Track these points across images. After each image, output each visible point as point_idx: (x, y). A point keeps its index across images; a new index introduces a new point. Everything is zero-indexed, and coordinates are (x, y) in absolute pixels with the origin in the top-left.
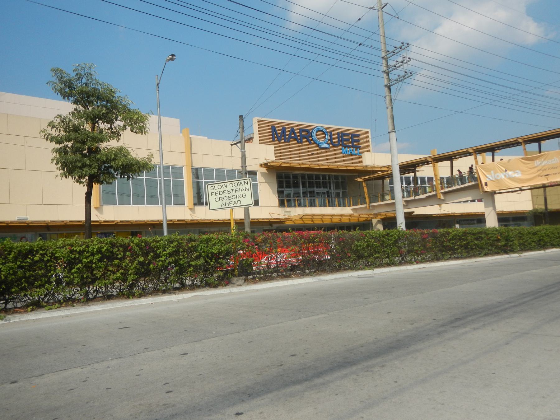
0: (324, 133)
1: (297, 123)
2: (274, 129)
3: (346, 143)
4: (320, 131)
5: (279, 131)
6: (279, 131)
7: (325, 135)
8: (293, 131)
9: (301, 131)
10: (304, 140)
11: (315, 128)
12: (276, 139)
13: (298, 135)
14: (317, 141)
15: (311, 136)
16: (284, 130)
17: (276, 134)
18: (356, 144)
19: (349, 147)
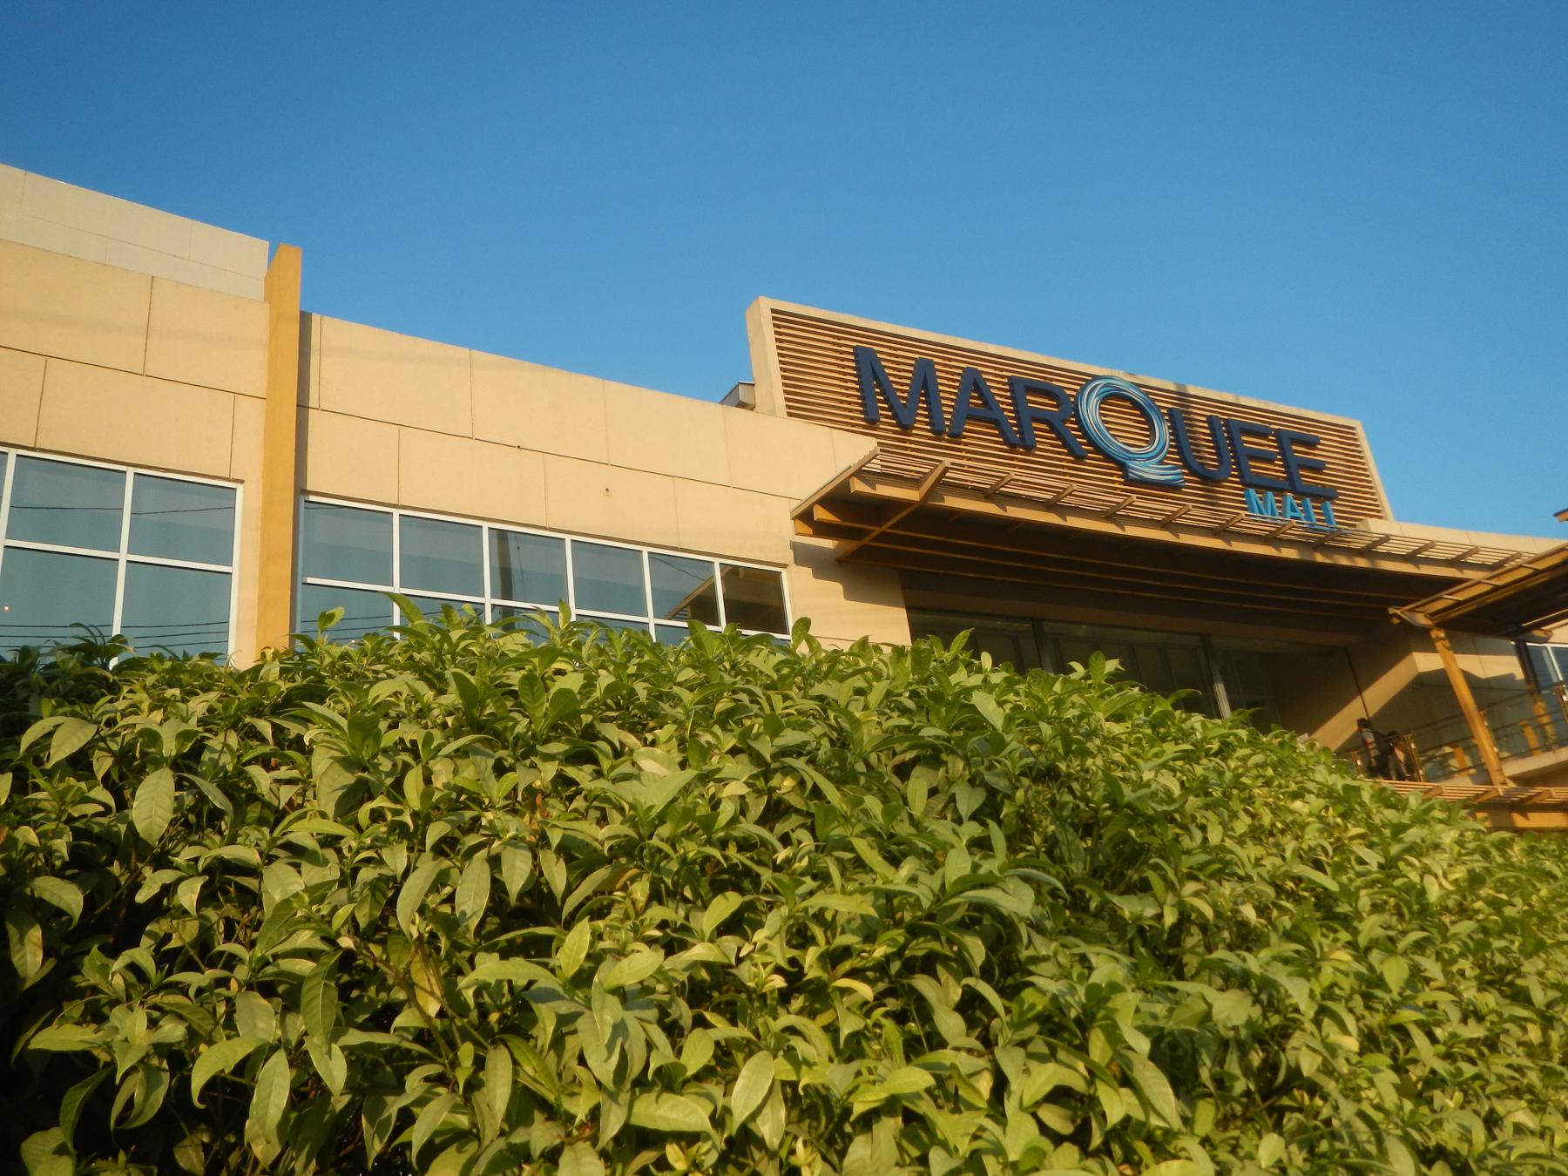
0: (1144, 413)
1: (992, 349)
2: (868, 368)
3: (1257, 468)
4: (1114, 397)
5: (901, 380)
6: (901, 380)
7: (1149, 421)
8: (973, 383)
9: (1022, 387)
10: (1045, 442)
11: (1091, 381)
12: (883, 409)
13: (1010, 411)
14: (1116, 445)
15: (1077, 415)
16: (924, 377)
17: (886, 401)
18: (1307, 477)
19: (1279, 491)
